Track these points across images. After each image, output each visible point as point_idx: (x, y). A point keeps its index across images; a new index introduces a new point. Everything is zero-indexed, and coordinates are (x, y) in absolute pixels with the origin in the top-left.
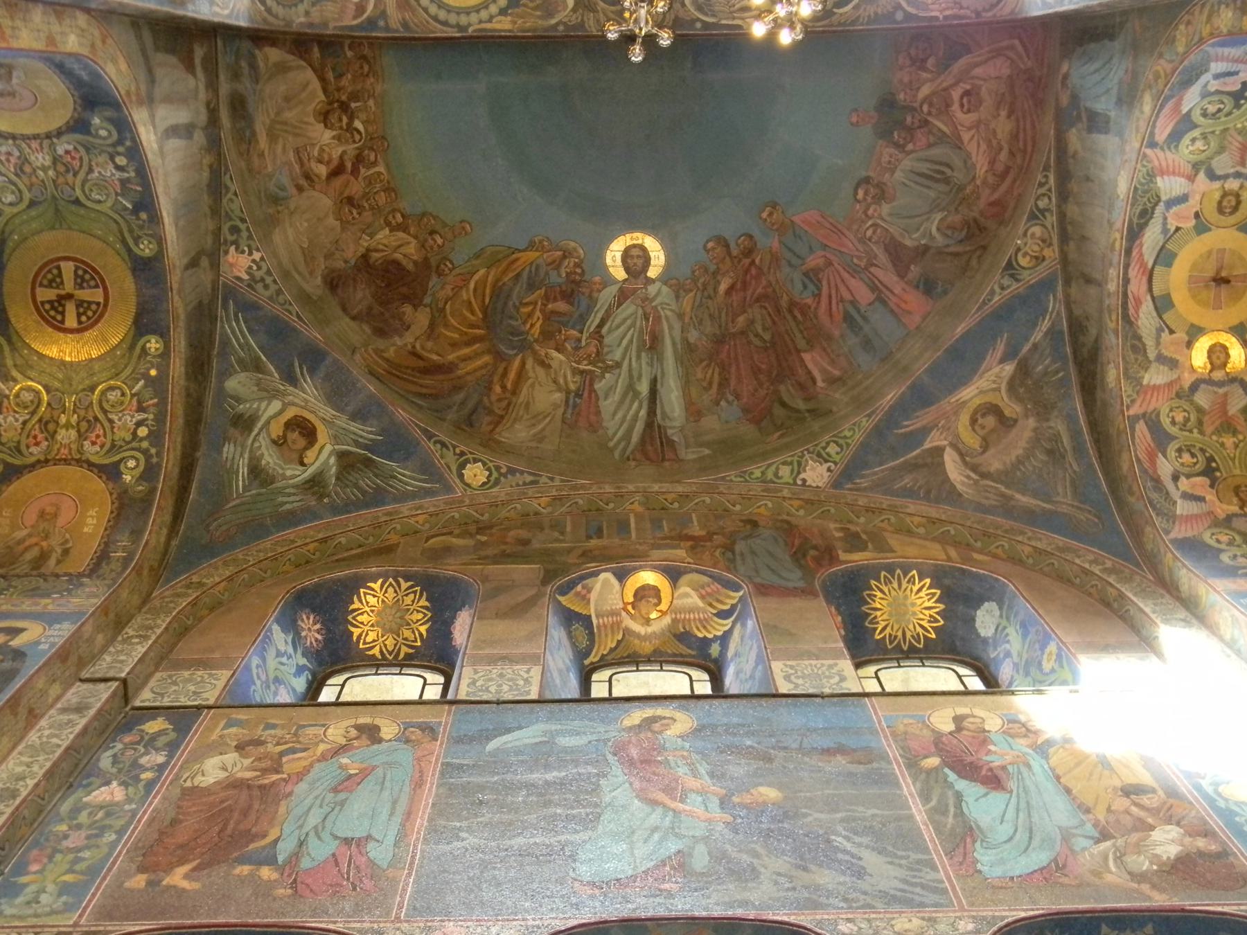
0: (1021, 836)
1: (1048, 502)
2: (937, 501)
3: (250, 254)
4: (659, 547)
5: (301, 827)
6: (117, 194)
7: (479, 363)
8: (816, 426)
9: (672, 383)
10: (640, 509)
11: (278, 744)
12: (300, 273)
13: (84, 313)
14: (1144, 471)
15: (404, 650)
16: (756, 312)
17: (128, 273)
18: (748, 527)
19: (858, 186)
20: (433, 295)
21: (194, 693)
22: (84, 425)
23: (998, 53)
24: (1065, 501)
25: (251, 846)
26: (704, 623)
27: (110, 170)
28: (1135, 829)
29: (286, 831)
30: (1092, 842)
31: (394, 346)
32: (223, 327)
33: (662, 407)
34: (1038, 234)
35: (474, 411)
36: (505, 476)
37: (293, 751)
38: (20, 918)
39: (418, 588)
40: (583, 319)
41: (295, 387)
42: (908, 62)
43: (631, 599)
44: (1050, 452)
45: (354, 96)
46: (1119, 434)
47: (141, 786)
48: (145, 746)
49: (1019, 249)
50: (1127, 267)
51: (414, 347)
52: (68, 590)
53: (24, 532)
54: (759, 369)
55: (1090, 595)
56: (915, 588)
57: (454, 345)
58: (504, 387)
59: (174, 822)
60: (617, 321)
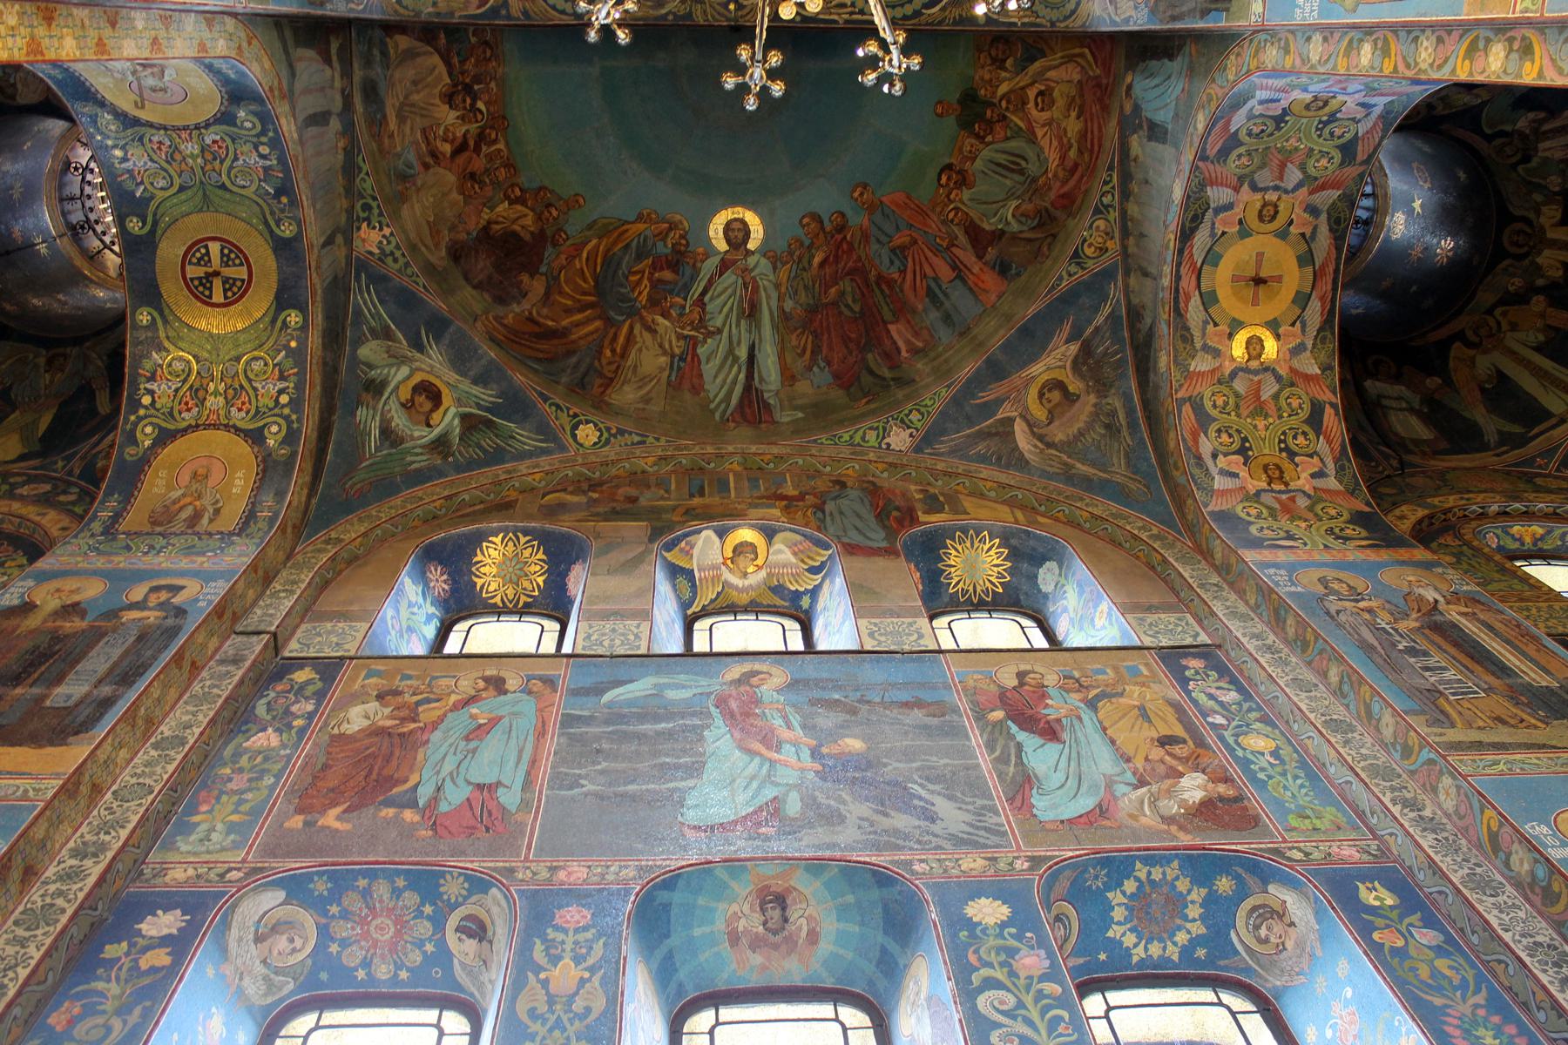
0: (1072, 783)
1: (1105, 471)
2: (1008, 466)
3: (381, 229)
4: (756, 506)
5: (438, 773)
6: (260, 180)
7: (591, 328)
8: (900, 394)
9: (769, 350)
10: (739, 469)
11: (414, 694)
12: (426, 246)
13: (230, 289)
14: (1188, 449)
15: (523, 599)
16: (846, 285)
17: (270, 252)
18: (837, 487)
19: (942, 171)
20: (548, 264)
21: (337, 644)
22: (231, 391)
23: (1070, 59)
24: (1119, 471)
25: (395, 790)
26: (796, 577)
27: (253, 159)
28: (1167, 776)
29: (425, 777)
30: (1130, 788)
31: (515, 311)
32: (355, 298)
33: (759, 372)
34: (1102, 228)
35: (585, 375)
36: (615, 436)
37: (428, 701)
38: (195, 854)
39: (536, 543)
40: (687, 288)
41: (422, 353)
42: (989, 62)
43: (730, 555)
44: (1107, 427)
45: (477, 79)
46: (1168, 414)
47: (294, 731)
48: (295, 695)
49: (1085, 241)
50: (1179, 265)
51: (530, 313)
52: (222, 549)
53: (180, 492)
54: (850, 338)
55: (1138, 558)
56: (986, 547)
57: (568, 311)
58: (613, 351)
59: (325, 767)
60: (719, 289)
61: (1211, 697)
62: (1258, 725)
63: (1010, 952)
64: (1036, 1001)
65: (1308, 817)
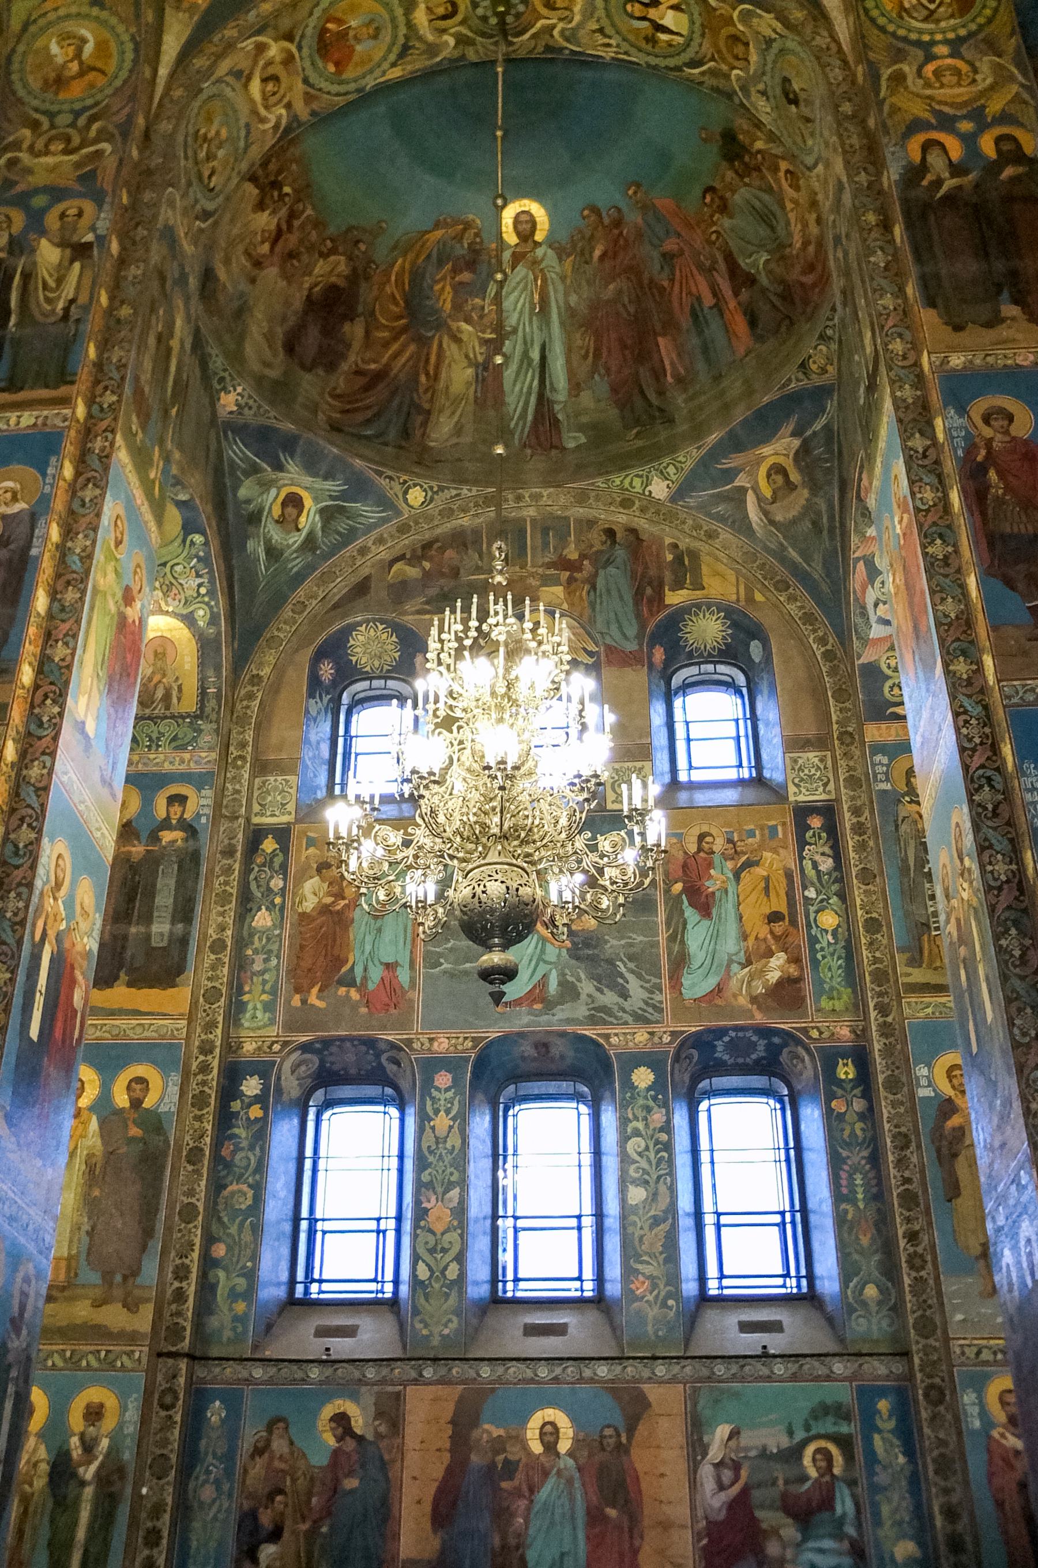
14: (856, 600)
15: (386, 667)
21: (283, 805)
22: (165, 588)
33: (551, 384)
36: (436, 493)
44: (814, 523)
49: (810, 357)
59: (302, 947)
60: (513, 284)
61: (815, 866)
62: (834, 900)
63: (649, 1110)
64: (655, 1145)
65: (833, 998)
